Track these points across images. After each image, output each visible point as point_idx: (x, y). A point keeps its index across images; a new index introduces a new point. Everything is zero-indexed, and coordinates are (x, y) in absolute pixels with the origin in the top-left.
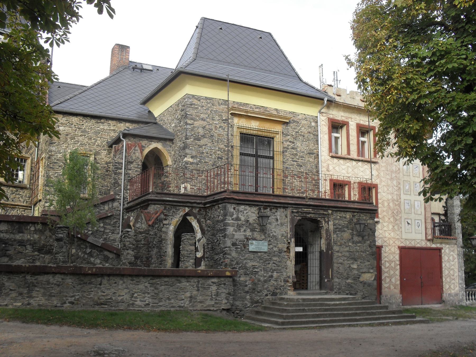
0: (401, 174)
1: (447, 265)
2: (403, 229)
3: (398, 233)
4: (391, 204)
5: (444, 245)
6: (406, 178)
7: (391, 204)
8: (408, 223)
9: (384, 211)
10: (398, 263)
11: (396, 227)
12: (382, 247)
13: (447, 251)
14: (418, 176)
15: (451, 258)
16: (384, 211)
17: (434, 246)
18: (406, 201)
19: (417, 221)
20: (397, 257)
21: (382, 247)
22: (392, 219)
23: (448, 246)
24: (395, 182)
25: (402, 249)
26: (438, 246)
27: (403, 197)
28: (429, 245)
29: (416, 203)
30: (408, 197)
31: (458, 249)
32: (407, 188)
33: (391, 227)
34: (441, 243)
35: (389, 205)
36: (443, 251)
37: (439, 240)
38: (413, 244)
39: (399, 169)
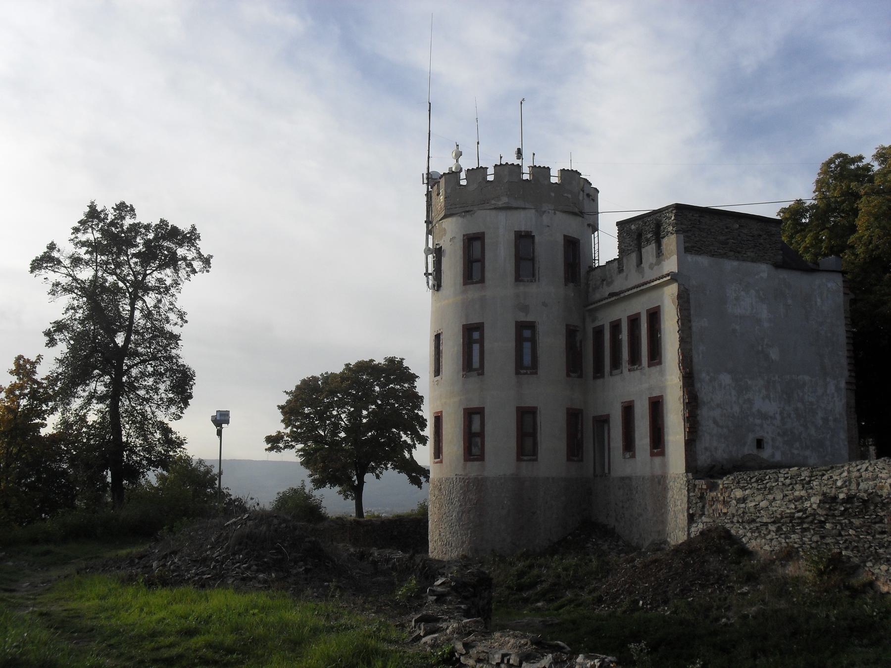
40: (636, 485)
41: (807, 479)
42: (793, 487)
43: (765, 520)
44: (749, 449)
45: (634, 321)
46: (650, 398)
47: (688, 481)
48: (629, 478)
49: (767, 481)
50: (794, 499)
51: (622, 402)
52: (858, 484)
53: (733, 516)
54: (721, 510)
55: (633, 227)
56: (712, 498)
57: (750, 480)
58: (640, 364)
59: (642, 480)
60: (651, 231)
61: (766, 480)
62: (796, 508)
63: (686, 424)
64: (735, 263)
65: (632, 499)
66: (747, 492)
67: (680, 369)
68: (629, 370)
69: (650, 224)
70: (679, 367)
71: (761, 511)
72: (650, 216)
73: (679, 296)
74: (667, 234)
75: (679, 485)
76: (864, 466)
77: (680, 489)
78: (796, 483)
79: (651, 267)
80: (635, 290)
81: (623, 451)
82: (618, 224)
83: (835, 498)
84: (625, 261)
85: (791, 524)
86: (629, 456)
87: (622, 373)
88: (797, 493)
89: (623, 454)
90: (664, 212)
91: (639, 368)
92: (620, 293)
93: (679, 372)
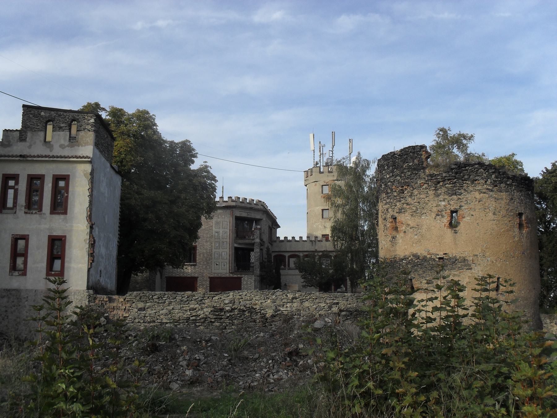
0: (213, 238)
1: (246, 286)
2: (213, 269)
3: (209, 270)
4: (205, 255)
5: (243, 276)
6: (216, 240)
7: (205, 255)
8: (217, 264)
9: (200, 259)
10: (208, 285)
11: (208, 267)
12: (198, 277)
13: (246, 279)
14: (226, 238)
15: (249, 283)
16: (200, 259)
17: (235, 276)
18: (215, 253)
19: (223, 263)
20: (208, 283)
21: (198, 277)
22: (205, 263)
23: (246, 276)
24: (209, 243)
25: (211, 278)
26: (239, 276)
27: (214, 250)
28: (231, 275)
29: (223, 253)
30: (217, 250)
31: (255, 277)
32: (217, 245)
33: (204, 267)
34: (241, 274)
35: (204, 255)
36: (242, 279)
37: (238, 273)
38: (220, 275)
39: (212, 236)
40: (26, 296)
41: (200, 299)
42: (189, 303)
43: (165, 321)
44: (98, 278)
45: (32, 178)
46: (49, 236)
47: (89, 296)
48: (18, 291)
49: (165, 298)
50: (190, 309)
51: (12, 235)
52: (240, 302)
53: (135, 319)
54: (123, 315)
55: (43, 113)
56: (114, 307)
57: (152, 297)
58: (40, 209)
59: (34, 292)
60: (66, 123)
61: (164, 297)
62: (190, 315)
63: (90, 257)
64: (104, 159)
65: (20, 305)
66: (148, 304)
67: (87, 221)
68: (26, 213)
69: (64, 118)
70: (87, 219)
71: (161, 316)
72: (66, 112)
73: (92, 173)
74: (84, 130)
75: (80, 298)
76: (244, 293)
77: (81, 299)
78: (192, 300)
79: (62, 147)
80: (47, 159)
81: (10, 269)
82: (24, 106)
83: (222, 310)
84: (29, 134)
85: (187, 324)
86: (18, 274)
87: (15, 213)
88: (192, 306)
89: (10, 272)
90: (82, 114)
91: (39, 213)
92: (28, 157)
93: (87, 223)
